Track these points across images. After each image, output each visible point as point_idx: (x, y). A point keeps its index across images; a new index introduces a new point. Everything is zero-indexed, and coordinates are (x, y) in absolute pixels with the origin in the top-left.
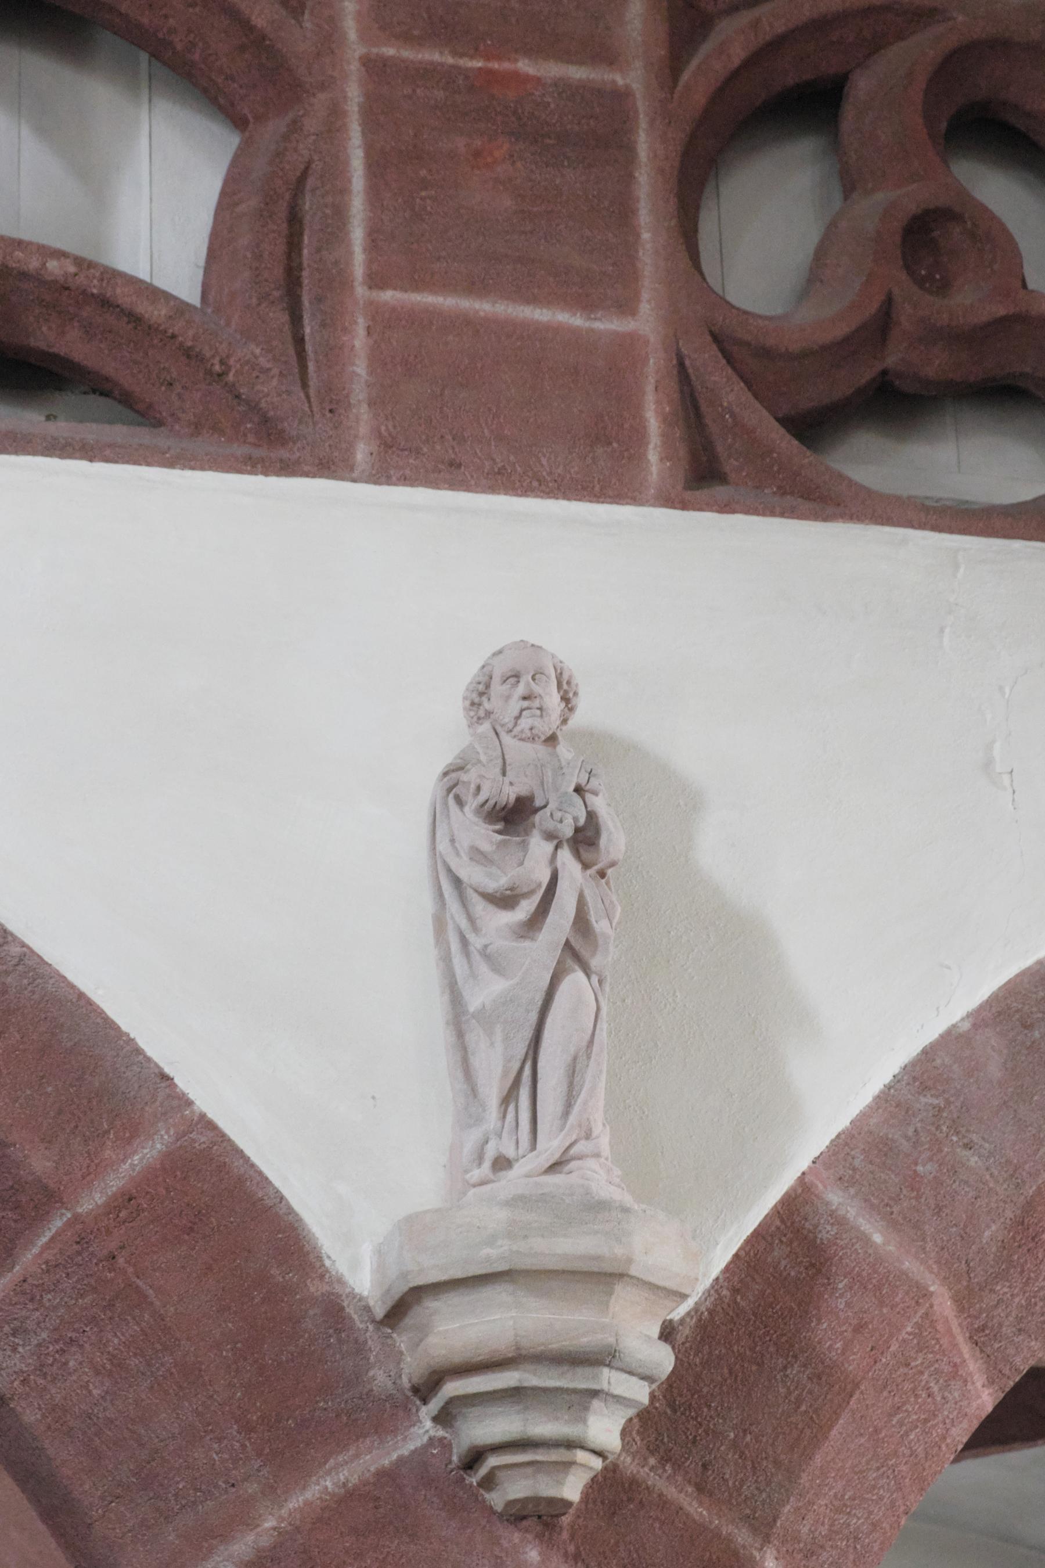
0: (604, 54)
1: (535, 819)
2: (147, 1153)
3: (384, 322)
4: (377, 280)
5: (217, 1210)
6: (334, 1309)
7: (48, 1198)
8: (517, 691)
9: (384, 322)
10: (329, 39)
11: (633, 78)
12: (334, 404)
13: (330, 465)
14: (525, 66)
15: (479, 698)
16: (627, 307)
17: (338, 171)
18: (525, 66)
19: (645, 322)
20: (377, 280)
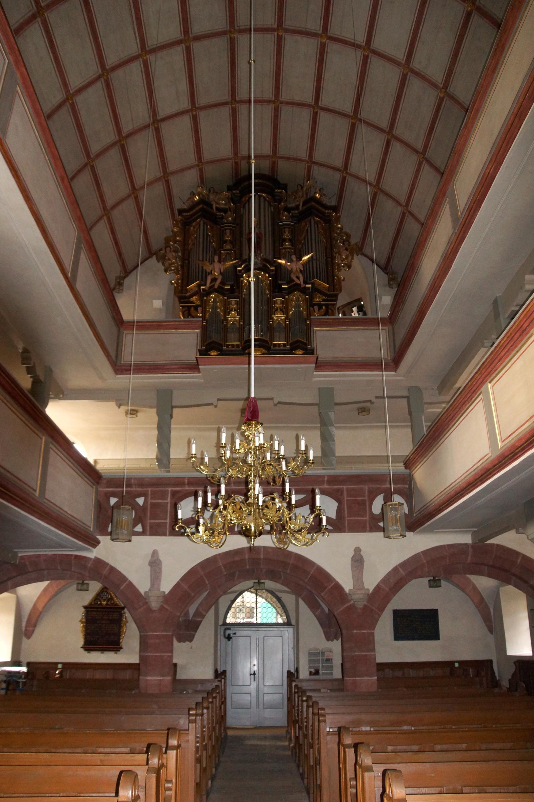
0: (364, 496)
1: (358, 561)
2: (333, 584)
3: (348, 520)
4: (348, 517)
5: (338, 587)
6: (346, 594)
7: (326, 587)
8: (357, 550)
9: (348, 520)
10: (344, 499)
11: (366, 498)
12: (344, 527)
13: (344, 532)
14: (358, 498)
15: (355, 550)
16: (366, 517)
17: (344, 509)
18: (358, 498)
19: (367, 518)
20: (348, 517)
